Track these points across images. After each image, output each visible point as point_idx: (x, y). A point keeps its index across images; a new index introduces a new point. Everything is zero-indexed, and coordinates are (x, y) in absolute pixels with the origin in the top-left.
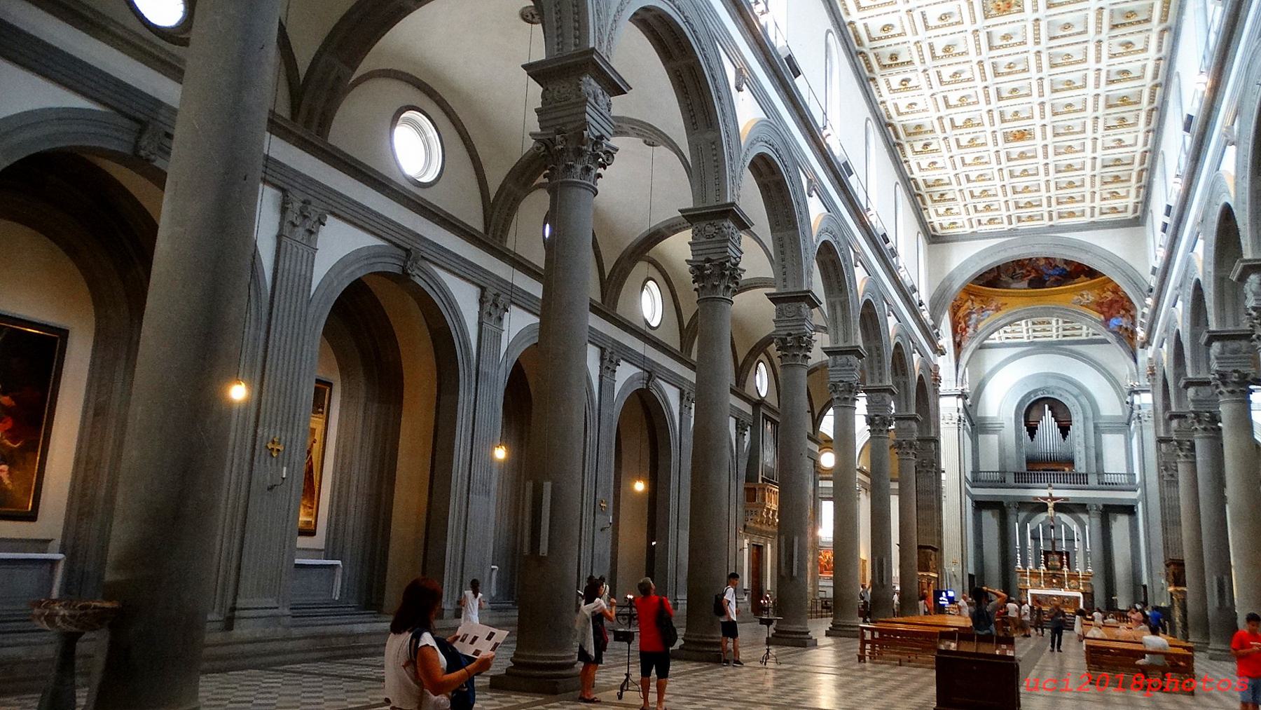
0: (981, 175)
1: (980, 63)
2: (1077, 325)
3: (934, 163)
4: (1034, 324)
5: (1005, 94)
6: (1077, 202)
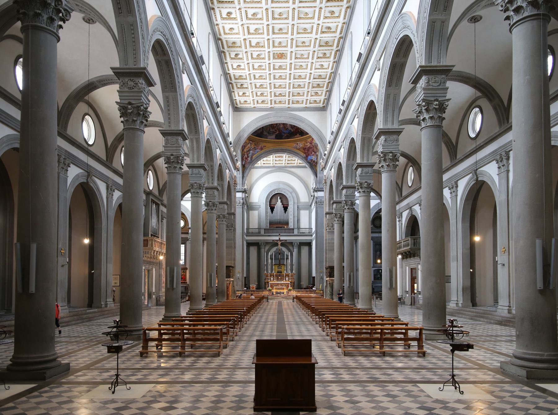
0: (261, 76)
1: (267, 9)
2: (294, 158)
3: (239, 66)
4: (276, 157)
5: (276, 31)
6: (301, 96)
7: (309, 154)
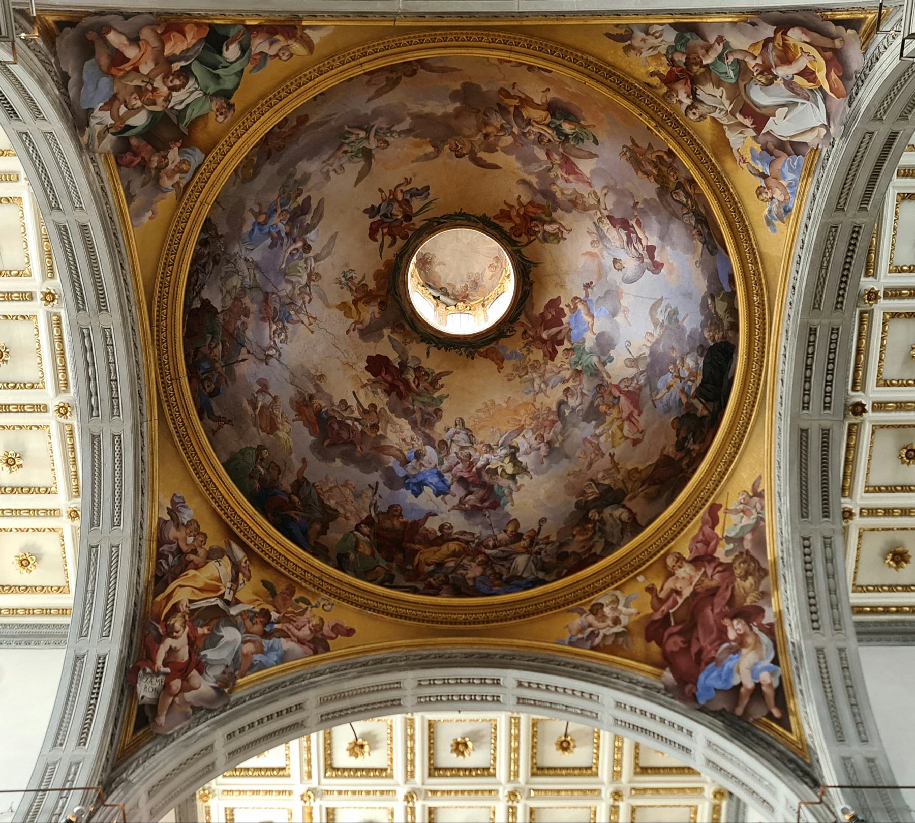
7: (700, 652)
